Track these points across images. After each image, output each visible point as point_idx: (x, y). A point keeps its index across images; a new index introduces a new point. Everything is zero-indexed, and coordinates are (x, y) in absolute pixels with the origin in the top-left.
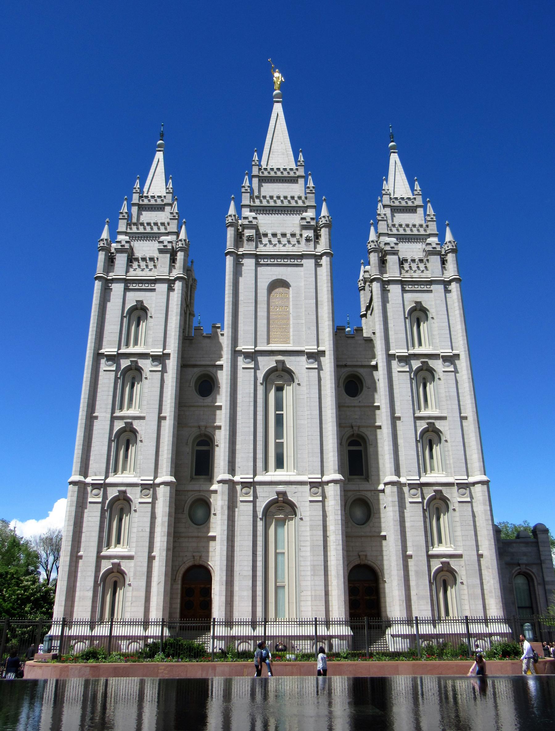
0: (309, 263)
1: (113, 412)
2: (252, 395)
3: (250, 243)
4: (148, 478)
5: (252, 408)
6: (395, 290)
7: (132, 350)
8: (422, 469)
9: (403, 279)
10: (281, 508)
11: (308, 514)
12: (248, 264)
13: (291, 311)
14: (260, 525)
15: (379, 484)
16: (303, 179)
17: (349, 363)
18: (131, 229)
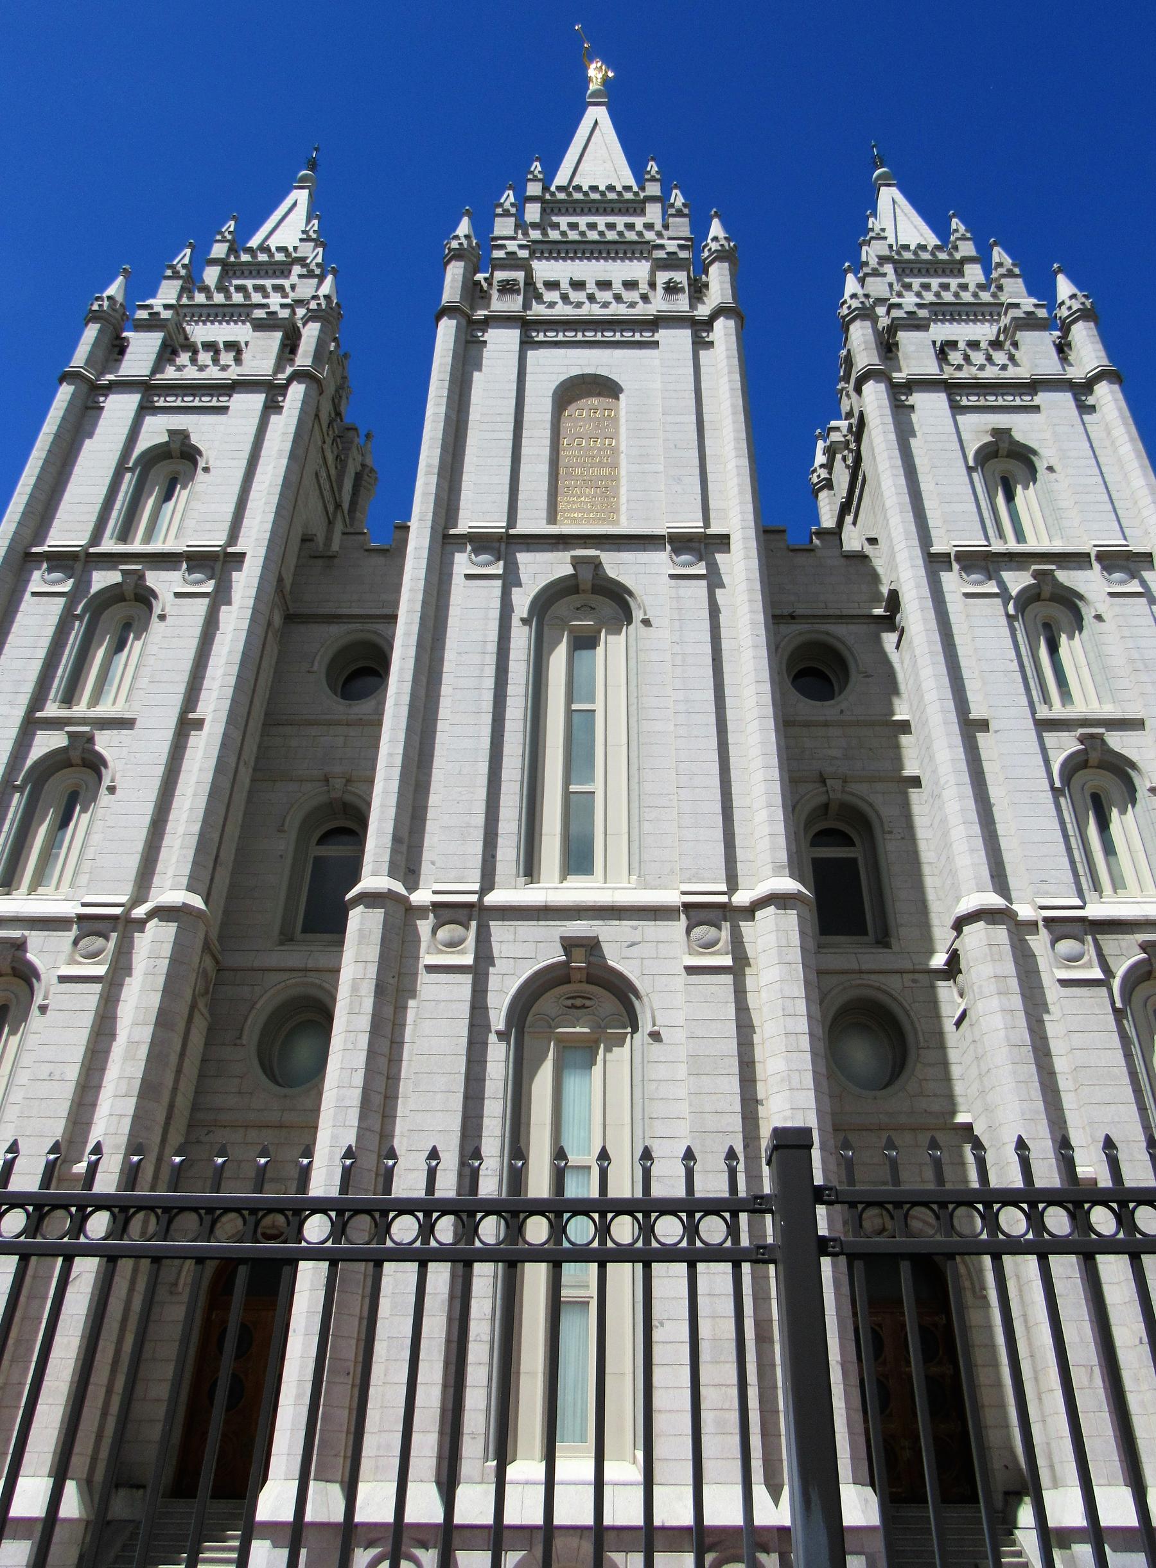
0: (677, 340)
1: (38, 699)
2: (492, 648)
3: (508, 296)
4: (112, 895)
5: (490, 683)
6: (930, 408)
8: (1086, 879)
10: (578, 1002)
11: (679, 1018)
12: (501, 344)
13: (623, 447)
14: (498, 1055)
15: (931, 952)
16: (659, 205)
18: (191, 298)
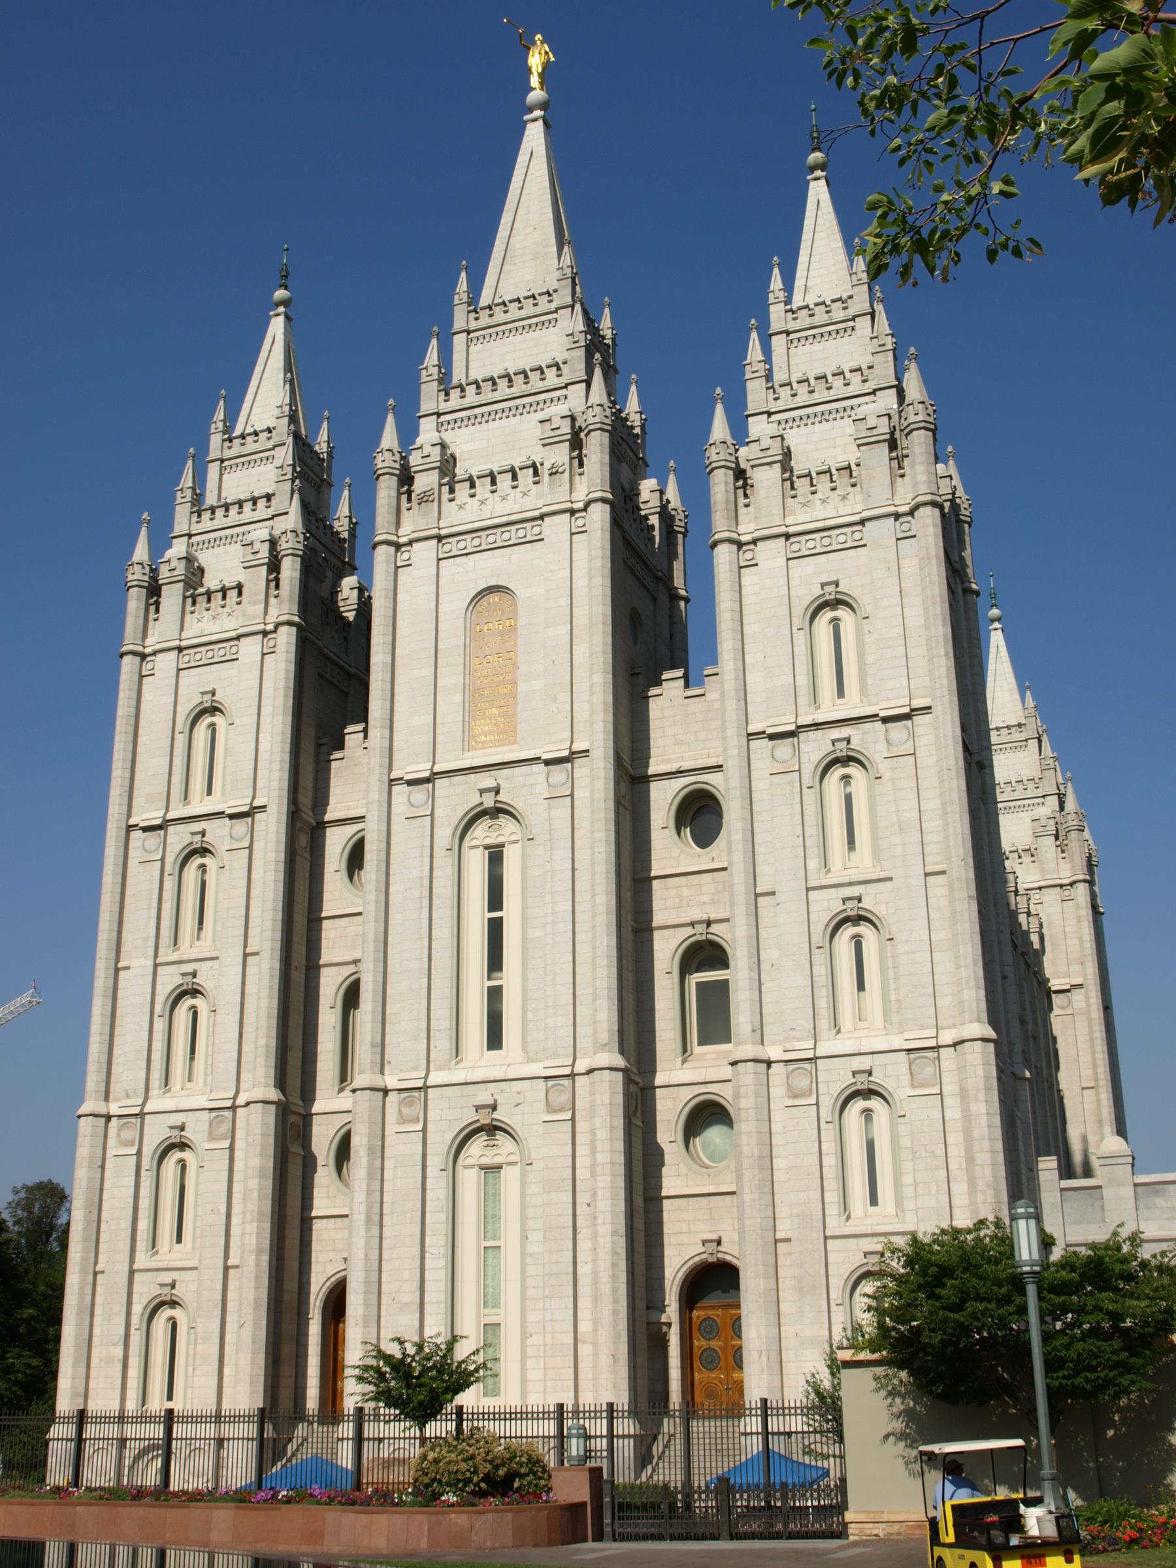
7: (197, 807)
9: (791, 530)
17: (686, 765)
